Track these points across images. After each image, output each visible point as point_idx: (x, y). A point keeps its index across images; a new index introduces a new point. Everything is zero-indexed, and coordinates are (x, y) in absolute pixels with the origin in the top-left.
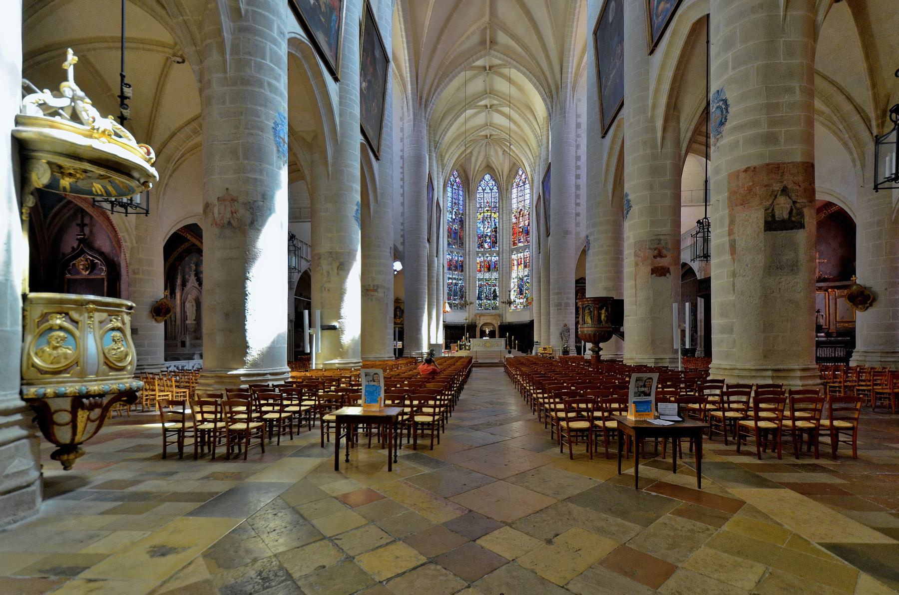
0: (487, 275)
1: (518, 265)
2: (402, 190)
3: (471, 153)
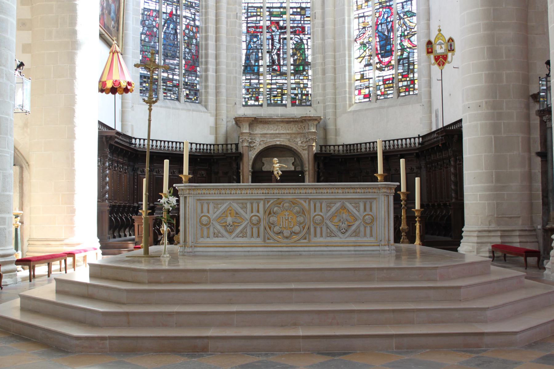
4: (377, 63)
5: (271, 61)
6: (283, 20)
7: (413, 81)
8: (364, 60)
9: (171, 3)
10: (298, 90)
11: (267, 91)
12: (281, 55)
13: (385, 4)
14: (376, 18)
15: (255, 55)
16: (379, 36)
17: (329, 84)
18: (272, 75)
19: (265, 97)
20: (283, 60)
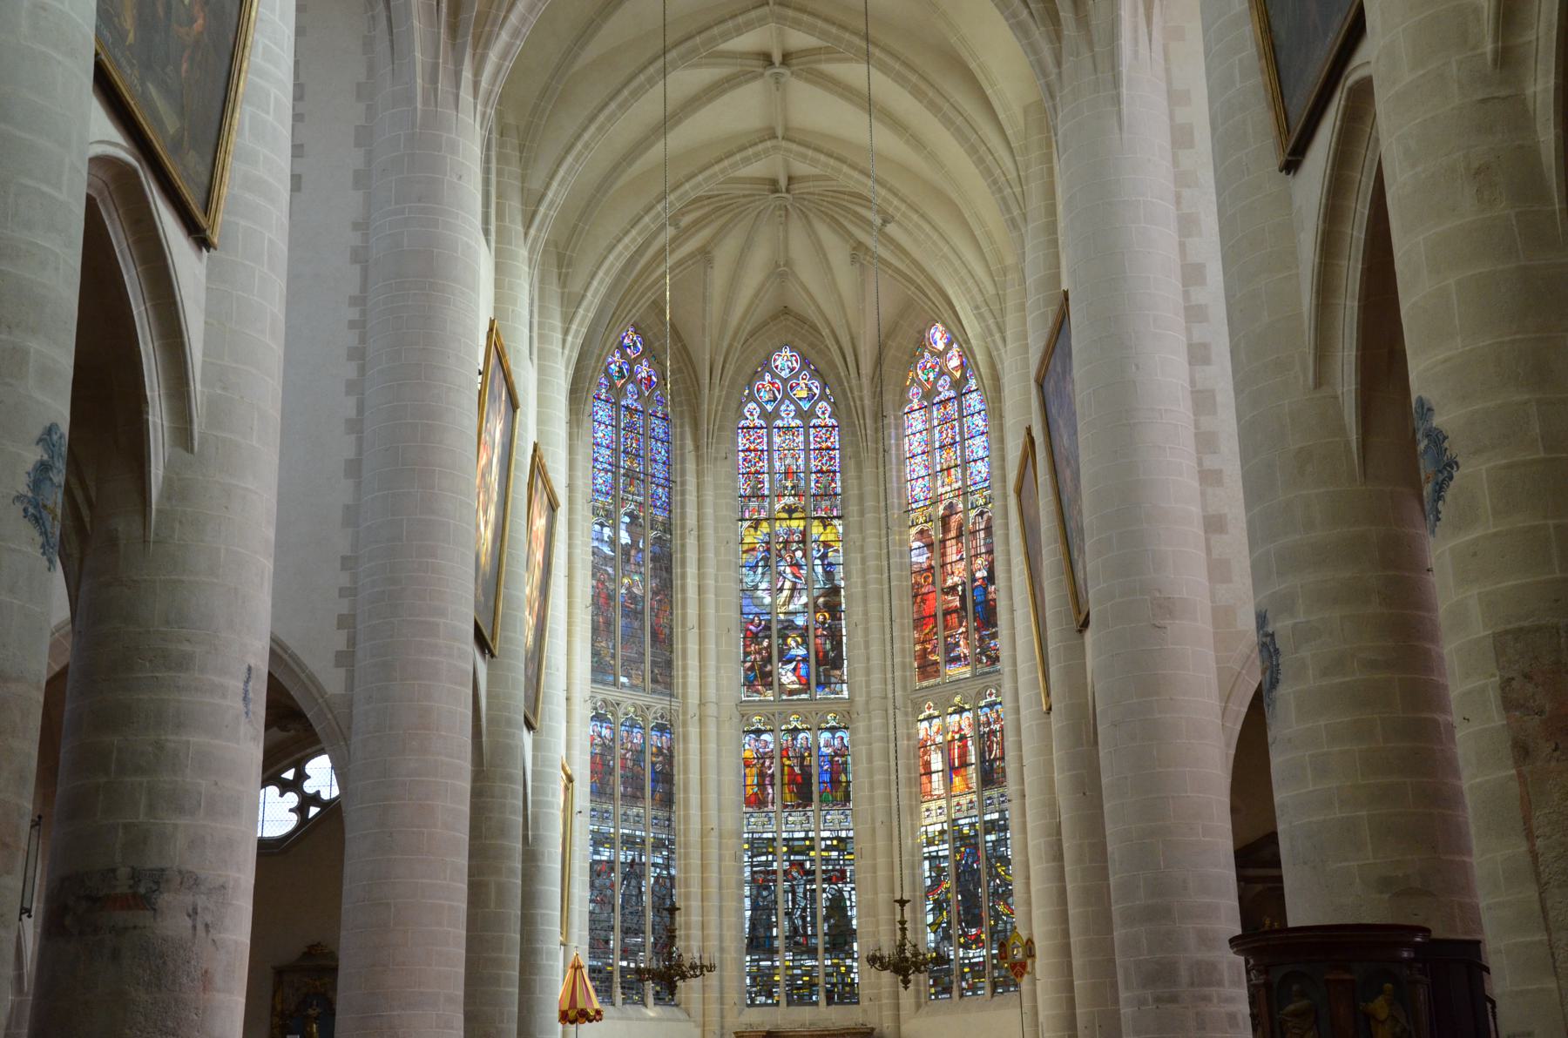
0: (794, 826)
1: (951, 770)
2: (351, 403)
3: (704, 255)
4: (960, 936)
12: (809, 919)
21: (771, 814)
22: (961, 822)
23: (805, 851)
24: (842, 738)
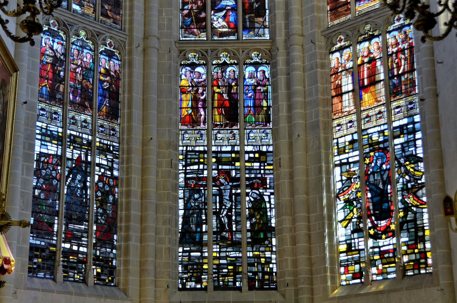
4: (370, 228)
5: (219, 225)
6: (236, 169)
7: (423, 253)
8: (351, 224)
9: (79, 146)
10: (257, 267)
11: (214, 269)
12: (234, 218)
13: (377, 146)
14: (365, 166)
15: (197, 217)
16: (371, 191)
17: (302, 258)
18: (220, 246)
19: (210, 276)
20: (236, 224)
21: (203, 132)
22: (370, 131)
23: (231, 162)
24: (264, 72)
